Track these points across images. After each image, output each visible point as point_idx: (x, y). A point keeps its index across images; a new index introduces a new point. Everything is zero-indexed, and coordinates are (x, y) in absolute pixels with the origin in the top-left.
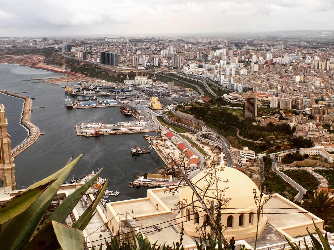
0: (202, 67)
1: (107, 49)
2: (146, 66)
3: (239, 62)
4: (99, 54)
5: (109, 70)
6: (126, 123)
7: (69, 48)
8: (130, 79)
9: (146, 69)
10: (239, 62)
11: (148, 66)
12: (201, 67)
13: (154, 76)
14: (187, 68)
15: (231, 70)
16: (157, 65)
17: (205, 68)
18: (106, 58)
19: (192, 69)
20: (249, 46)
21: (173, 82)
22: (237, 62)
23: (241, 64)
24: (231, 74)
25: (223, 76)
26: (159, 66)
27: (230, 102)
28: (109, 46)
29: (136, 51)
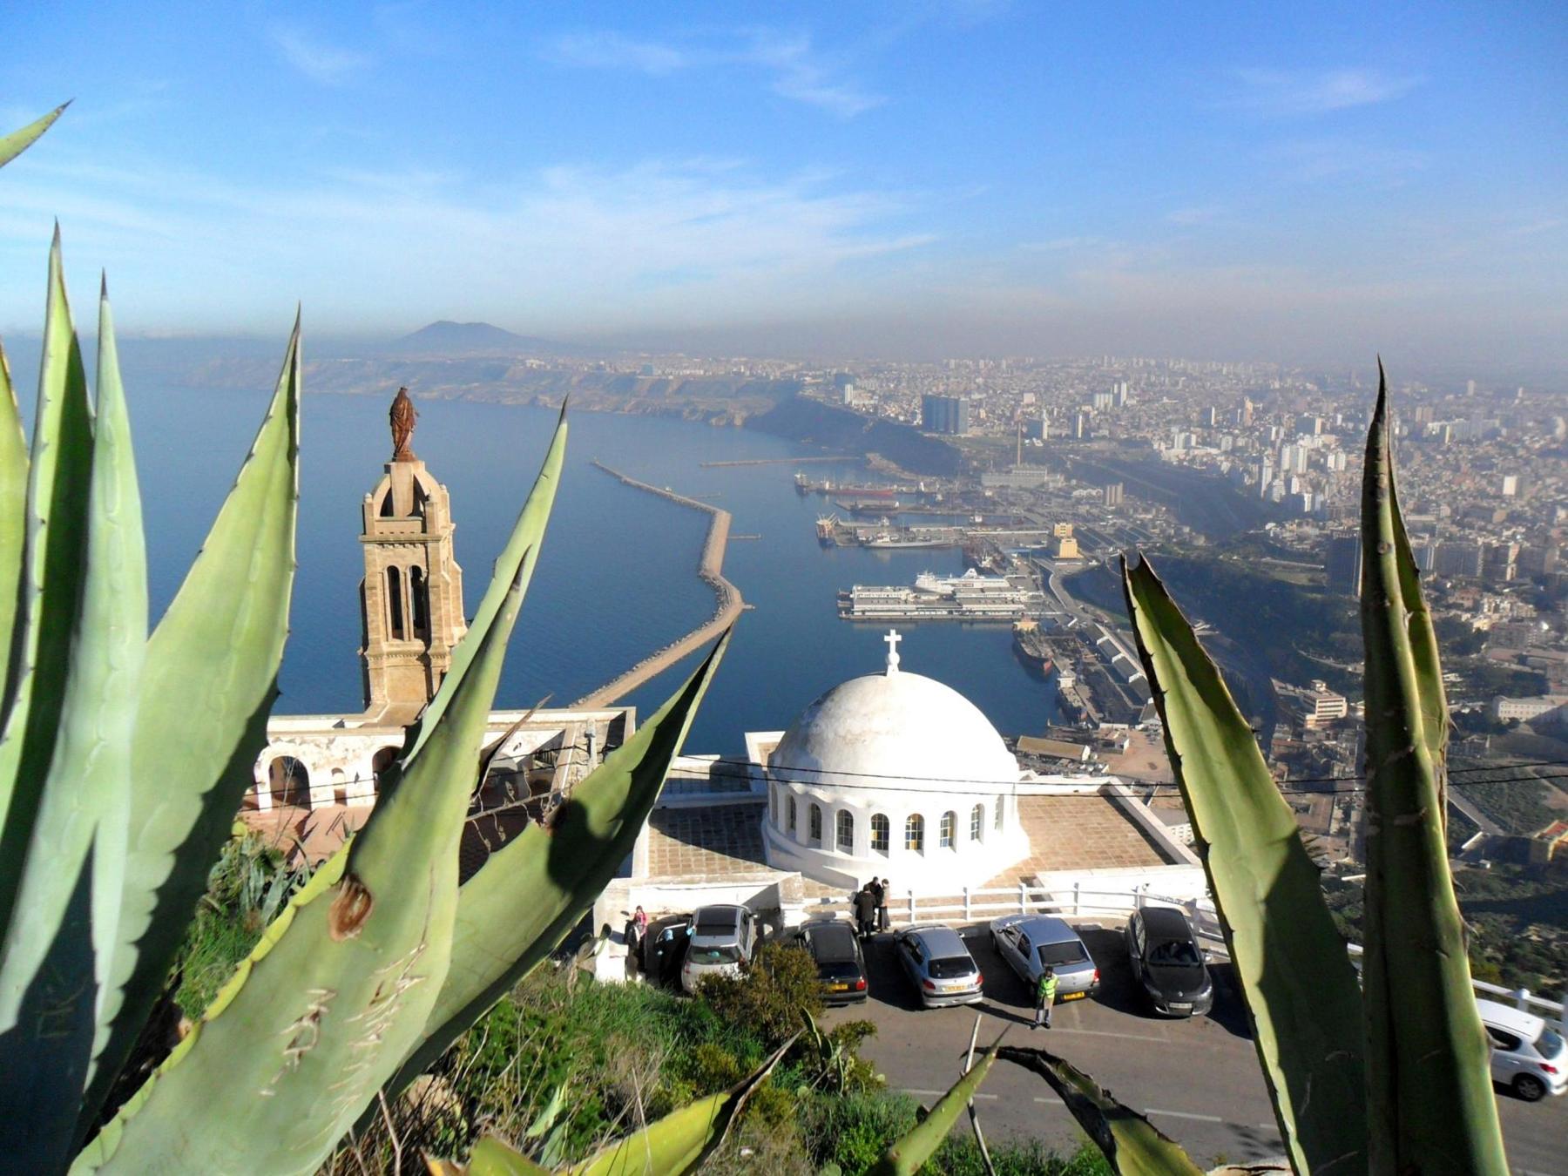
0: (1210, 445)
1: (941, 388)
4: (917, 401)
7: (841, 380)
10: (1323, 431)
11: (1054, 436)
12: (1204, 443)
14: (1163, 447)
15: (1294, 455)
17: (1218, 446)
18: (940, 411)
19: (1175, 449)
21: (1120, 488)
22: (1318, 429)
23: (1331, 439)
24: (1294, 463)
26: (1086, 437)
29: (1022, 393)
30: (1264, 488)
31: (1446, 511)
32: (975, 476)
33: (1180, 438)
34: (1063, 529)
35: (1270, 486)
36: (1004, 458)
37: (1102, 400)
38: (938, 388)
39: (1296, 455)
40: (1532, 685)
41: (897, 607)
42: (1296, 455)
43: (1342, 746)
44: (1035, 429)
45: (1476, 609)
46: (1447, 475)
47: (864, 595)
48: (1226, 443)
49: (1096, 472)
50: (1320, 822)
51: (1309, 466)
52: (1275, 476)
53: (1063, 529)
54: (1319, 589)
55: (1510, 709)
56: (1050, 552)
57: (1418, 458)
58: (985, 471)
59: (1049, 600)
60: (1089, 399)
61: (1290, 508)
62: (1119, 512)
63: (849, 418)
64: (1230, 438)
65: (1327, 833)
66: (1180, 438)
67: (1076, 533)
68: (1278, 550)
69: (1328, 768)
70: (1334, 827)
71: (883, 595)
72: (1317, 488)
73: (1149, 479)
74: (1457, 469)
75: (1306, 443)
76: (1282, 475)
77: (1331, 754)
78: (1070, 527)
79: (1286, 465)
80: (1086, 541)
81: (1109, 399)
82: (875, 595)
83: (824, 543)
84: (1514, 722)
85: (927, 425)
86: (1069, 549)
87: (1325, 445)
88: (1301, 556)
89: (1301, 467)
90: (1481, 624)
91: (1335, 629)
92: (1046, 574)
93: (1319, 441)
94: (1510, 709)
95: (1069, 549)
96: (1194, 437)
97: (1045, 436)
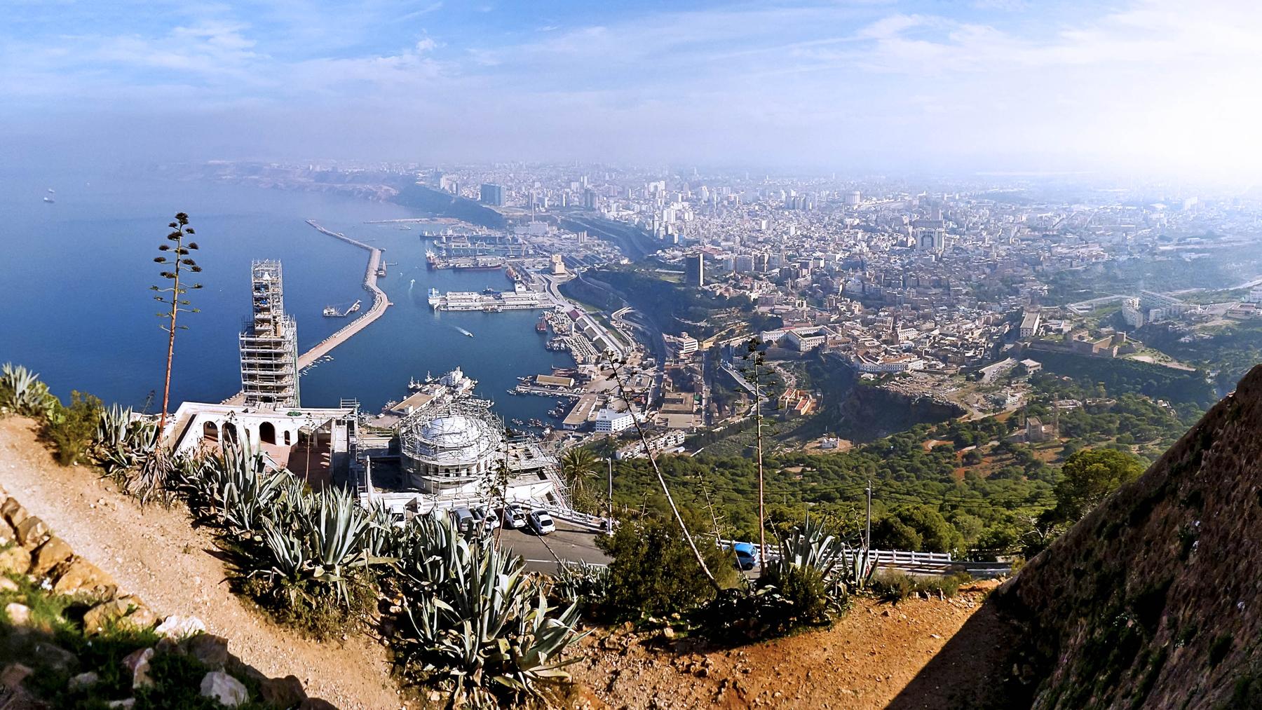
18: (490, 192)
23: (686, 204)
25: (657, 224)
31: (738, 239)
33: (614, 206)
34: (557, 258)
36: (524, 221)
37: (575, 185)
38: (489, 180)
39: (670, 215)
40: (776, 323)
42: (670, 215)
43: (696, 366)
44: (541, 201)
45: (751, 290)
46: (738, 221)
48: (637, 208)
49: (573, 227)
50: (688, 407)
53: (557, 258)
54: (684, 285)
55: (767, 336)
56: (550, 271)
57: (725, 212)
60: (568, 183)
61: (668, 242)
62: (586, 247)
63: (442, 196)
65: (691, 412)
66: (614, 206)
67: (563, 259)
69: (691, 379)
70: (695, 409)
72: (680, 230)
73: (600, 229)
74: (742, 217)
75: (676, 206)
77: (692, 370)
80: (569, 263)
81: (577, 184)
84: (770, 342)
85: (483, 200)
86: (560, 268)
88: (674, 267)
89: (673, 220)
90: (754, 296)
92: (550, 282)
94: (767, 336)
95: (560, 268)
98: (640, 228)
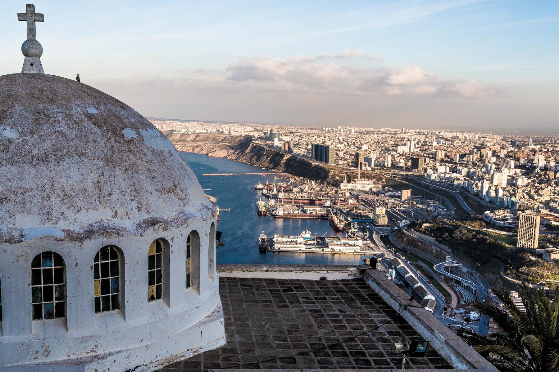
0: (456, 172)
2: (373, 166)
3: (516, 167)
5: (322, 169)
6: (335, 241)
8: (349, 182)
9: (373, 169)
10: (516, 167)
12: (453, 170)
13: (384, 180)
16: (389, 166)
17: (460, 172)
18: (321, 152)
20: (535, 145)
22: (512, 166)
23: (518, 171)
27: (494, 223)
28: (325, 137)
29: (362, 145)
30: (484, 193)
32: (336, 184)
35: (488, 192)
39: (501, 179)
41: (296, 246)
47: (280, 239)
51: (508, 185)
52: (490, 188)
58: (342, 182)
59: (372, 245)
64: (467, 170)
68: (490, 224)
71: (290, 240)
76: (493, 188)
78: (384, 210)
79: (495, 183)
82: (285, 239)
83: (259, 213)
87: (515, 174)
89: (504, 184)
91: (523, 265)
93: (512, 173)
96: (448, 168)
97: (373, 166)
98: (465, 191)
